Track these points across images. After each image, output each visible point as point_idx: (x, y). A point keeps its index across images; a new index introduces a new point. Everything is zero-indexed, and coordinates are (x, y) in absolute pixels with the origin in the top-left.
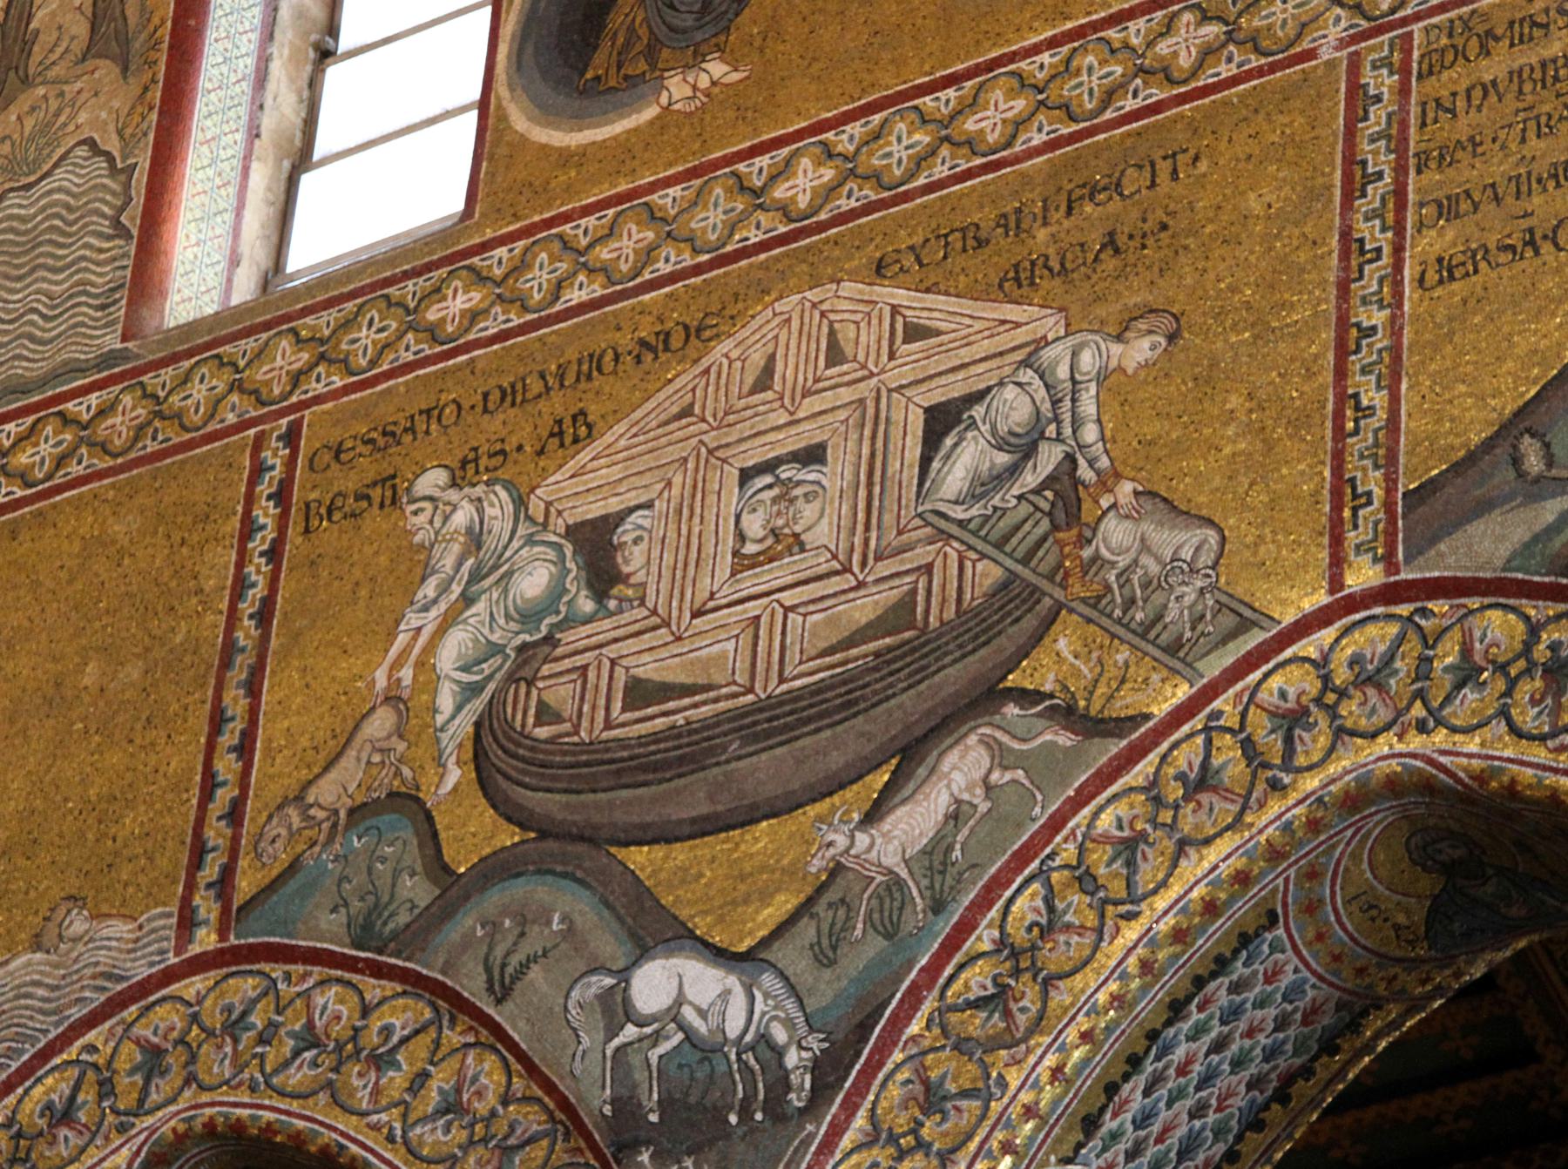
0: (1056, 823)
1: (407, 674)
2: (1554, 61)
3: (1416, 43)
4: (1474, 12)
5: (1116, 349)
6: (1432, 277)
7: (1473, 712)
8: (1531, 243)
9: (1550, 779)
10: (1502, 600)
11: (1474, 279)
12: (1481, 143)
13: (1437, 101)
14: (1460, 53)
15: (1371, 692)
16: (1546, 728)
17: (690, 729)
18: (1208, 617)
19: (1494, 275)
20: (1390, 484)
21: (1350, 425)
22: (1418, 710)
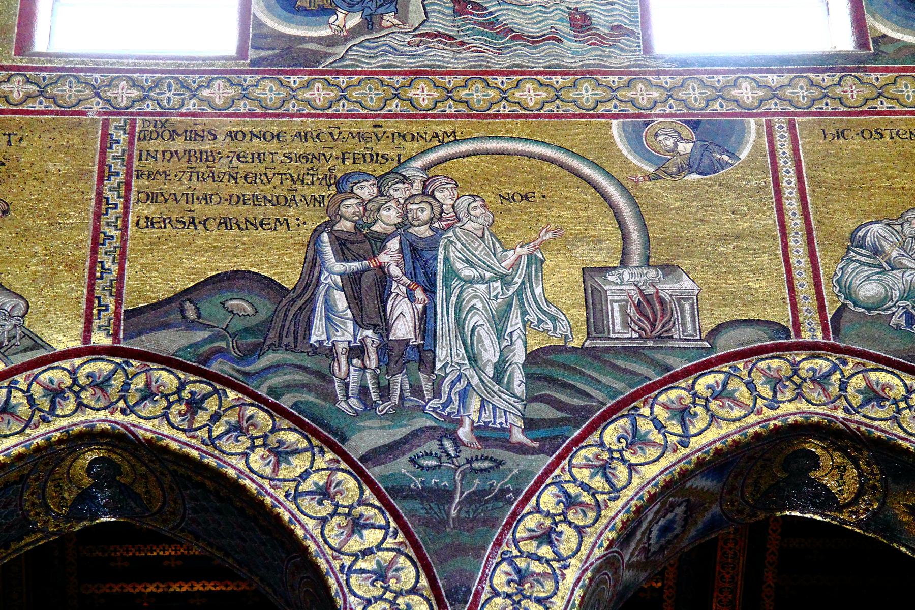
2: (207, 152)
3: (137, 125)
4: (167, 121)
6: (143, 223)
7: (150, 411)
8: (193, 223)
9: (186, 450)
10: (168, 368)
11: (164, 230)
12: (169, 175)
13: (148, 151)
14: (160, 135)
15: (97, 390)
16: (186, 427)
18: (18, 337)
19: (174, 231)
20: (118, 304)
21: (98, 275)
22: (121, 404)
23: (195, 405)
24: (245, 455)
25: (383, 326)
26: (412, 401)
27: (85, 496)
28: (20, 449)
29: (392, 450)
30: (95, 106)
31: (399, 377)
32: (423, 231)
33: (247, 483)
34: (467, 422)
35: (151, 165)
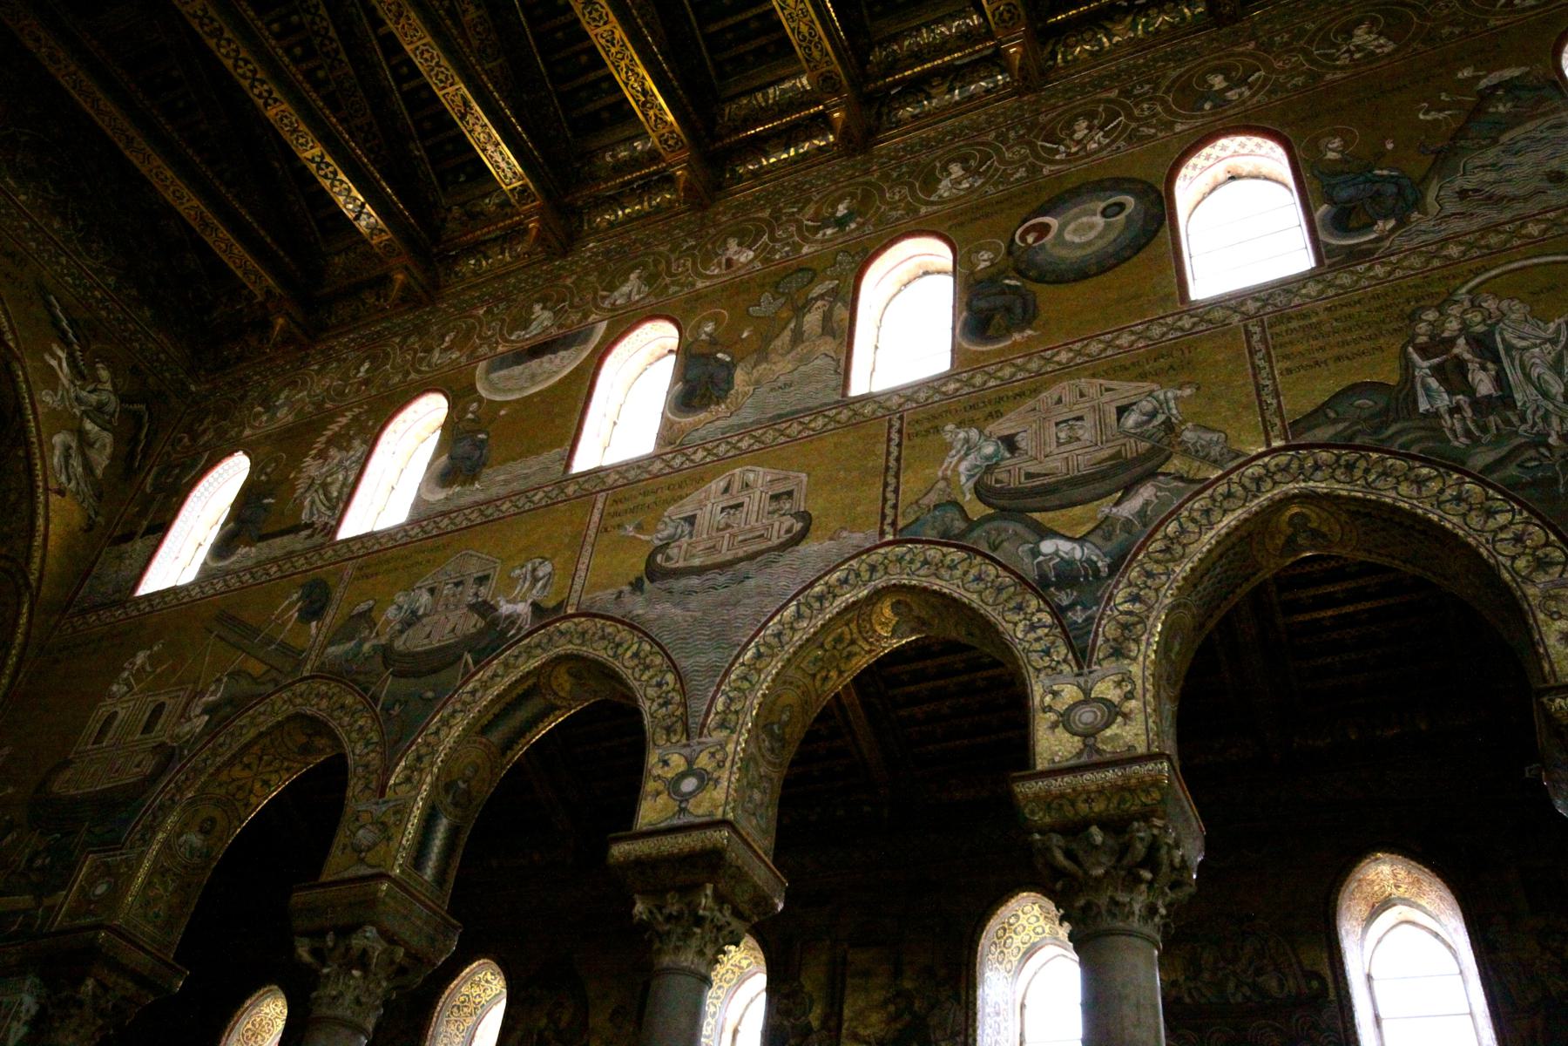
0: (1181, 506)
1: (949, 473)
5: (1179, 392)
17: (1049, 484)
20: (1283, 421)
23: (1350, 467)
24: (1395, 488)
25: (1470, 390)
26: (1505, 429)
27: (1291, 541)
28: (1245, 515)
29: (1500, 463)
30: (1236, 318)
31: (1491, 418)
32: (1480, 328)
33: (1402, 504)
34: (1553, 433)
35: (1280, 340)
